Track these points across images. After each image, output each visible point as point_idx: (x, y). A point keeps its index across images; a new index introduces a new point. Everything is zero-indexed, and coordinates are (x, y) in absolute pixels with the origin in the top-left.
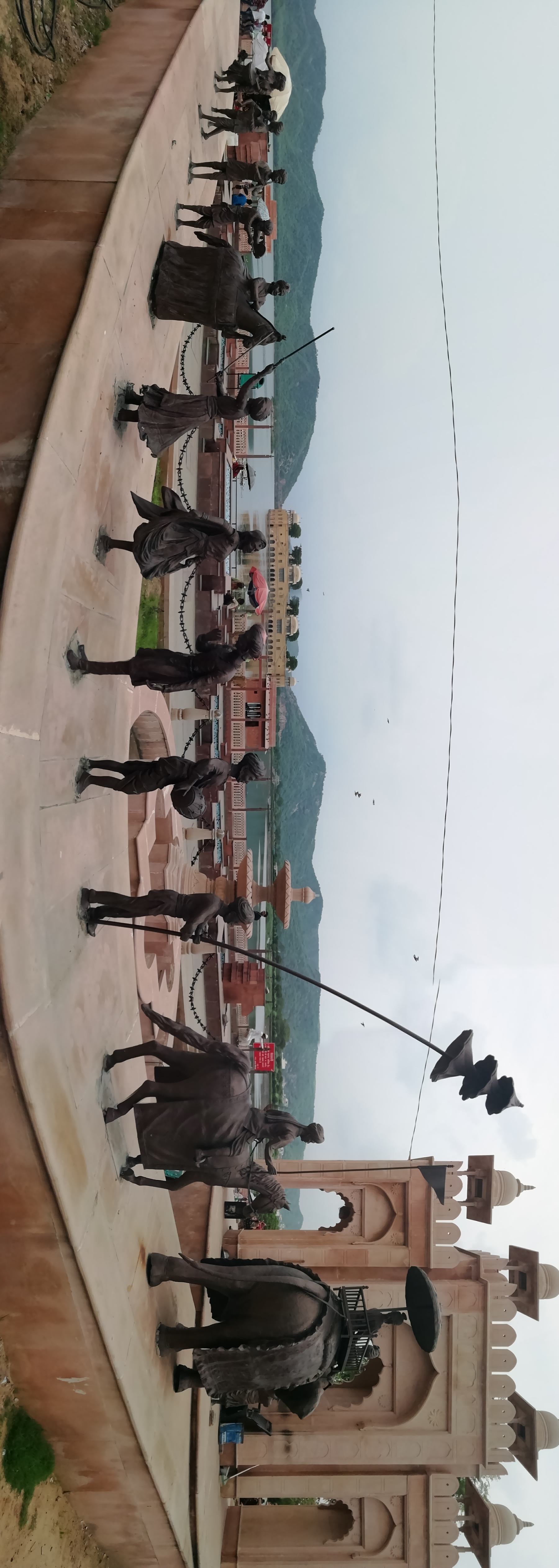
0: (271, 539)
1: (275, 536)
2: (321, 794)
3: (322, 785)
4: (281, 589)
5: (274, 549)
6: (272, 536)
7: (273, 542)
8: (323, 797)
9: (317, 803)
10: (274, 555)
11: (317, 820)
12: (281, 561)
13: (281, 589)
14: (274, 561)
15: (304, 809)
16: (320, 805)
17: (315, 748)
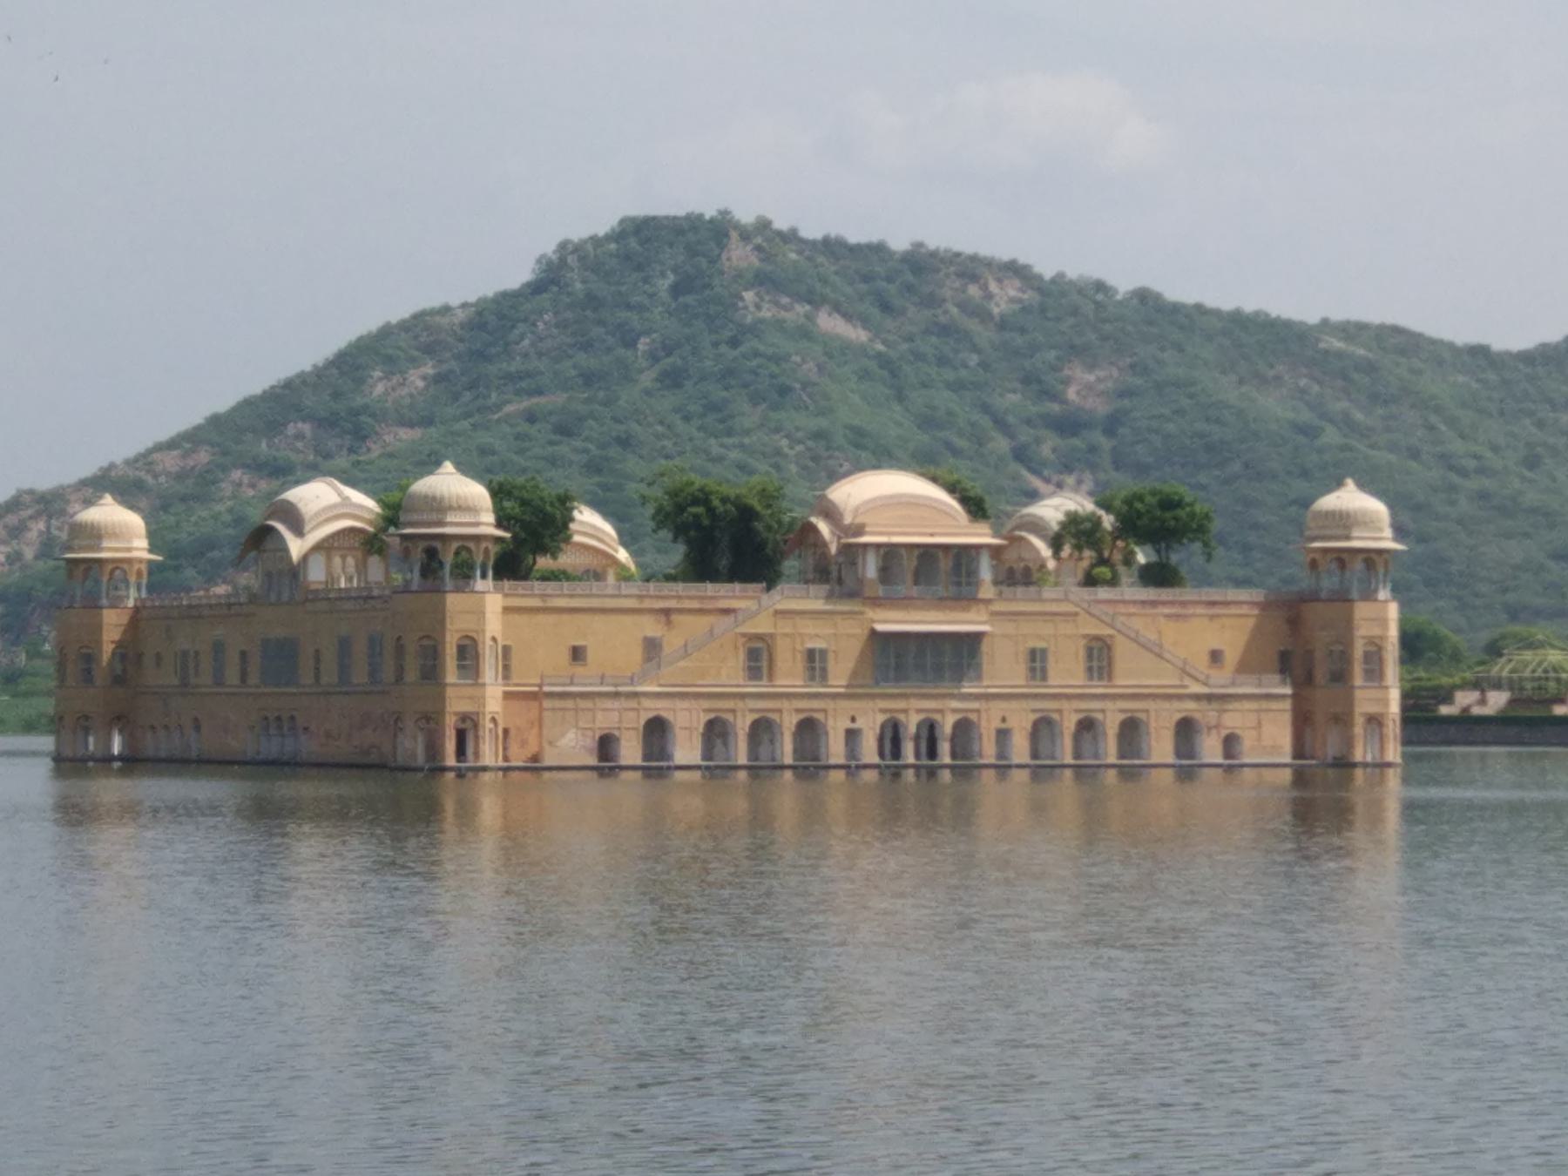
0: (630, 751)
1: (606, 718)
2: (921, 265)
3: (832, 247)
4: (1037, 662)
5: (716, 732)
6: (606, 745)
7: (657, 730)
8: (936, 240)
9: (1004, 297)
10: (762, 729)
11: (1149, 305)
12: (815, 662)
13: (1037, 662)
14: (809, 729)
15: (1068, 425)
16: (1014, 270)
17: (495, 321)
